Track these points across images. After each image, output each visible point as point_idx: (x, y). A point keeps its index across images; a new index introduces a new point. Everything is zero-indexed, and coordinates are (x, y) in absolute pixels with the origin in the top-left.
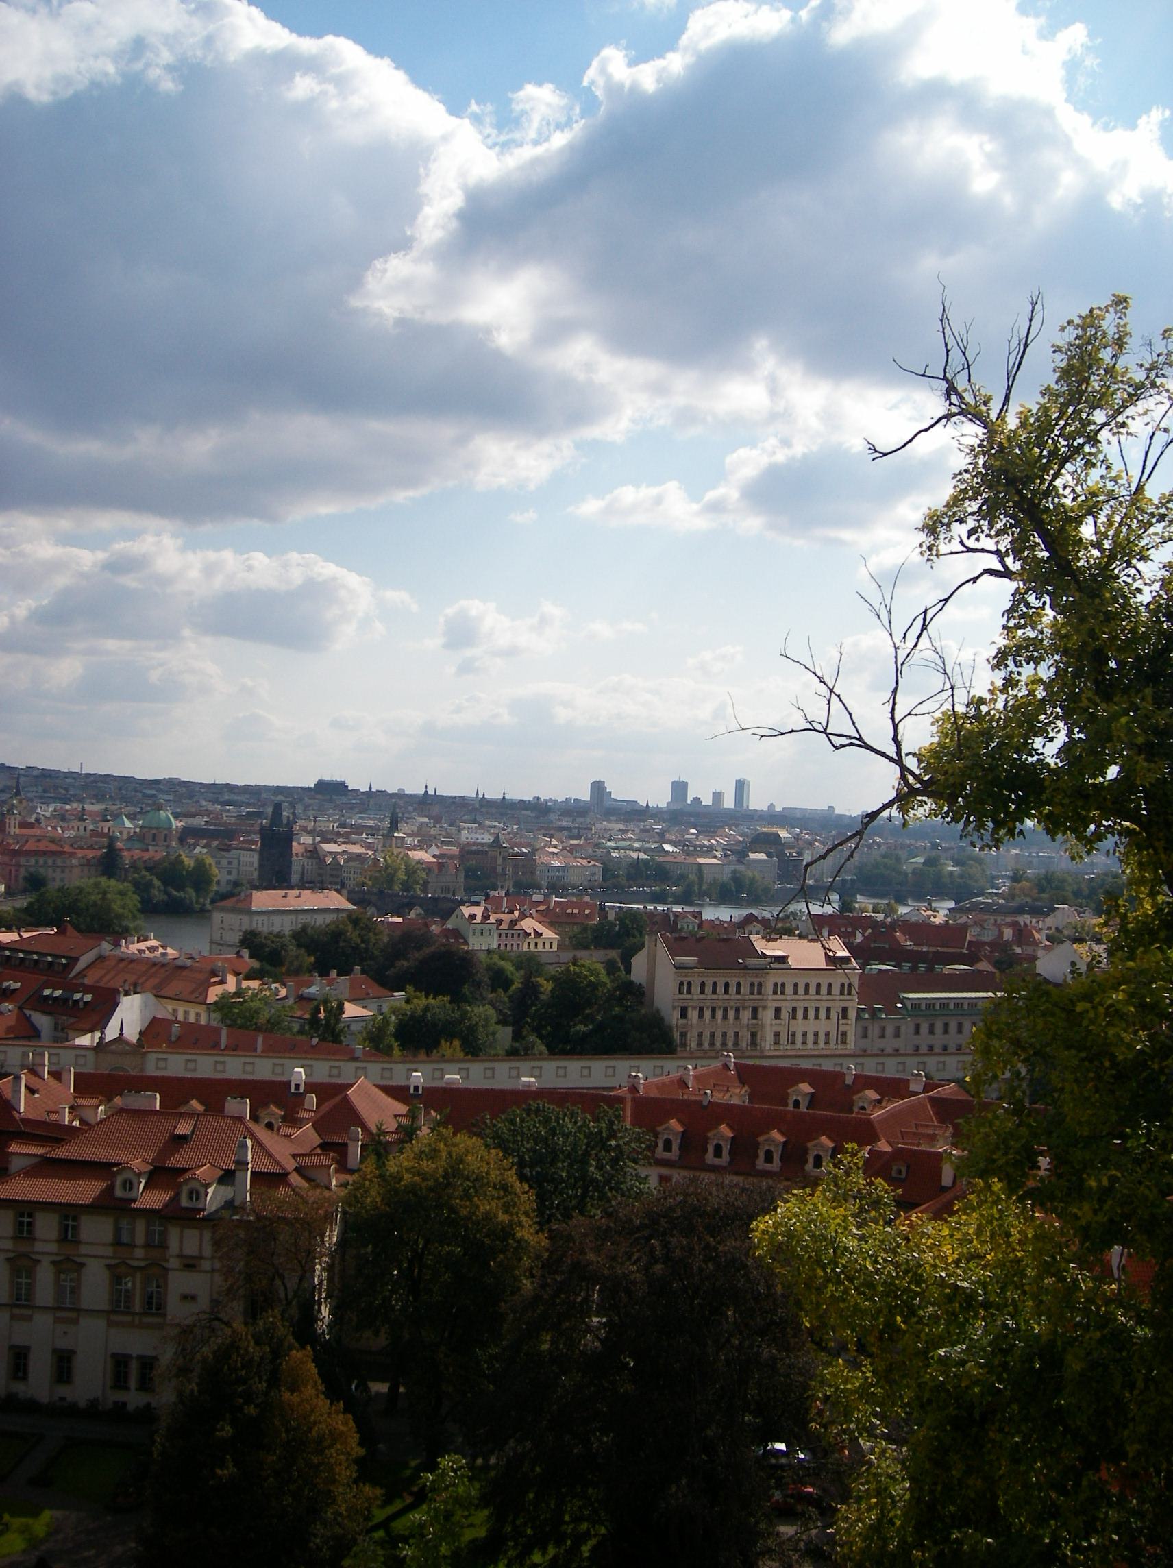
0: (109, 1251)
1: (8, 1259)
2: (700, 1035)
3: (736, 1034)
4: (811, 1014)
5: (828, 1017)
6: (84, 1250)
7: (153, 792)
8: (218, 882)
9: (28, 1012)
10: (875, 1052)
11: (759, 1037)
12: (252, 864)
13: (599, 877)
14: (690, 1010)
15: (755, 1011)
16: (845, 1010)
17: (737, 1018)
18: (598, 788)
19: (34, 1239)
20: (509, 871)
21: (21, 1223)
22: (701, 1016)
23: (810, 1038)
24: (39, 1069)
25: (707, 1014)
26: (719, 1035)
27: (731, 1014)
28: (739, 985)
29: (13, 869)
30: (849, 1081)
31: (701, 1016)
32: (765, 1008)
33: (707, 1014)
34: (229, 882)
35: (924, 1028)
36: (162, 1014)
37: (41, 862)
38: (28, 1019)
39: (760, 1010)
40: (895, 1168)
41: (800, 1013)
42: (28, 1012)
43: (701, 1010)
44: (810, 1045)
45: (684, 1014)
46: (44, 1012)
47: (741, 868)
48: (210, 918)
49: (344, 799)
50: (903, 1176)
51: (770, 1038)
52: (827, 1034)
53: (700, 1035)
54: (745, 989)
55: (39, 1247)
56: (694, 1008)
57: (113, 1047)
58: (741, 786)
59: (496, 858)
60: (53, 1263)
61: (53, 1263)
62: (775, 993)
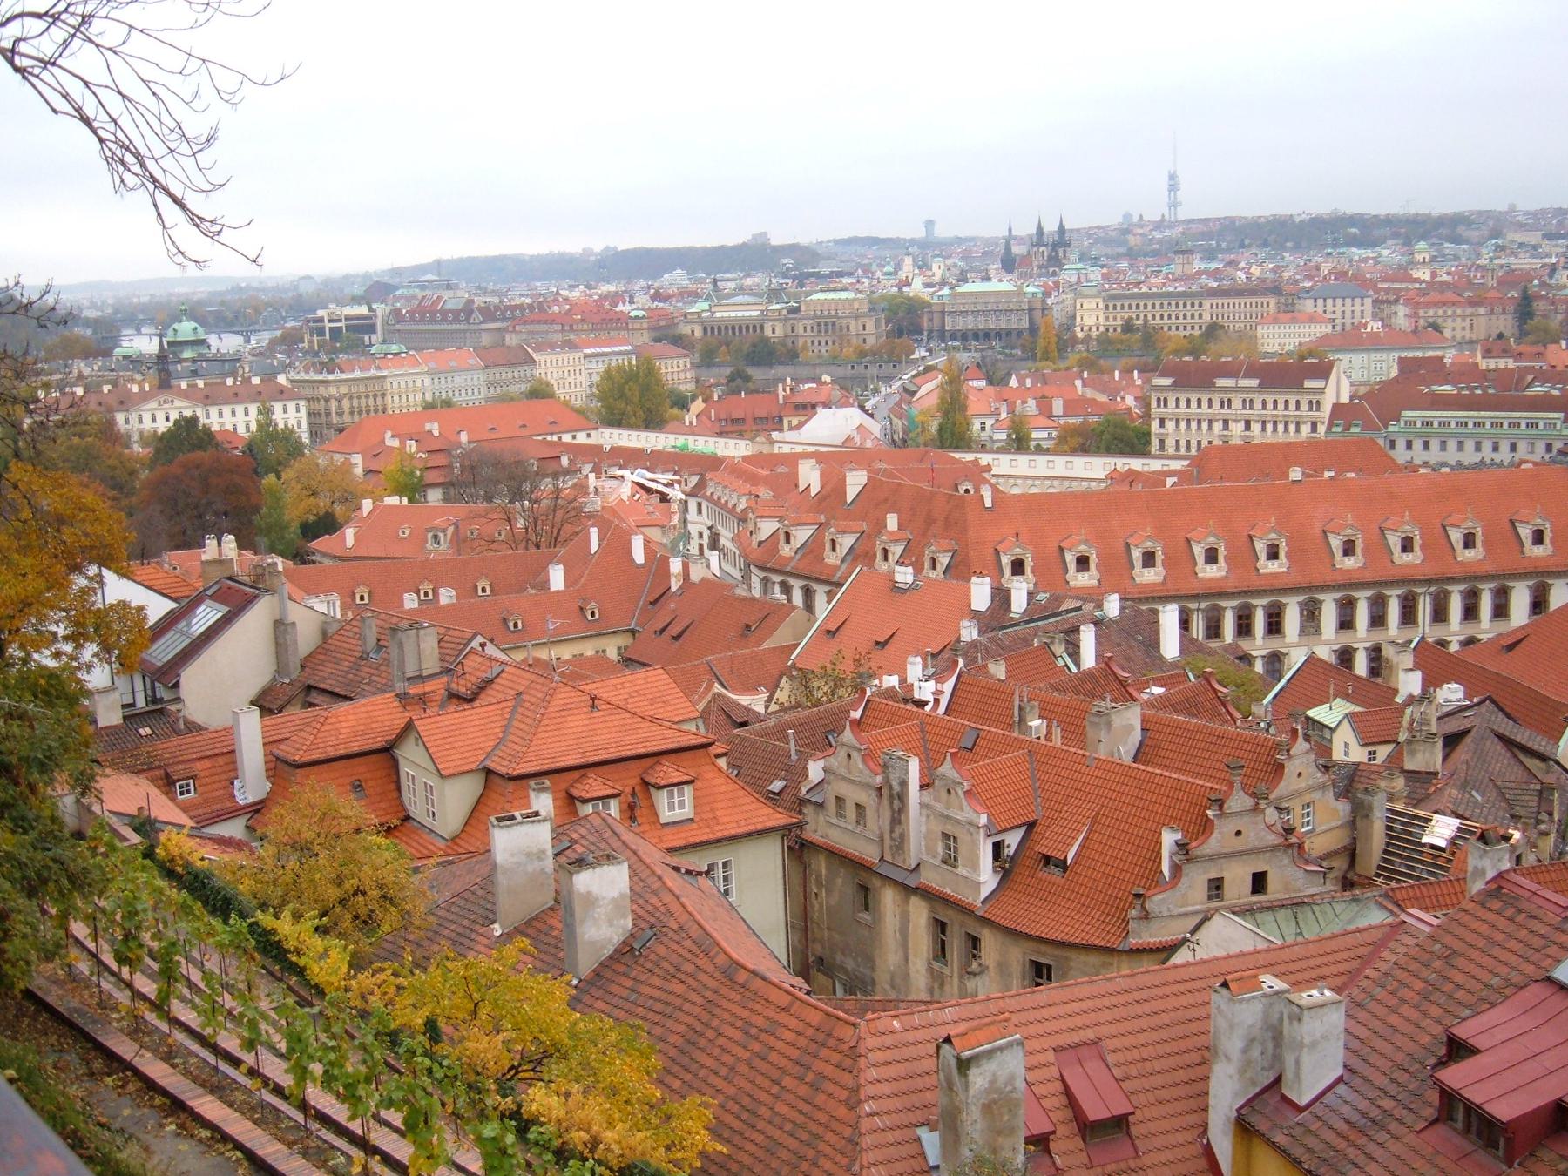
15: (1226, 422)
17: (1210, 428)
25: (1183, 425)
27: (1205, 426)
29: (1413, 320)
33: (1183, 425)
37: (1440, 312)
41: (1269, 427)
43: (1178, 421)
45: (1162, 422)
53: (1178, 442)
54: (1216, 405)
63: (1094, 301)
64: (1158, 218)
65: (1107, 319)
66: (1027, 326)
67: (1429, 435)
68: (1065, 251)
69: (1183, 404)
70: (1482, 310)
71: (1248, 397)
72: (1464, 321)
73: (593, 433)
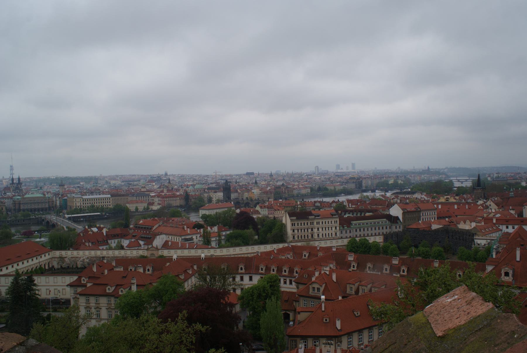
0: (106, 305)
1: (85, 308)
2: (298, 236)
3: (308, 235)
4: (327, 229)
5: (332, 229)
6: (101, 305)
7: (207, 178)
8: (213, 201)
9: (138, 241)
10: (345, 237)
11: (314, 235)
12: (222, 195)
13: (309, 191)
14: (295, 230)
15: (312, 230)
16: (336, 227)
17: (308, 231)
18: (317, 167)
19: (90, 303)
20: (286, 192)
21: (87, 299)
22: (298, 231)
23: (327, 234)
24: (104, 261)
25: (300, 231)
26: (306, 235)
27: (306, 230)
28: (307, 223)
30: (318, 249)
31: (298, 231)
32: (315, 228)
33: (300, 231)
34: (216, 200)
35: (358, 230)
36: (168, 239)
38: (139, 242)
39: (313, 229)
40: (305, 275)
41: (324, 229)
42: (138, 241)
44: (327, 236)
45: (294, 231)
46: (142, 241)
47: (346, 186)
48: (199, 211)
49: (253, 176)
50: (307, 277)
51: (316, 235)
52: (332, 234)
53: (298, 236)
54: (309, 224)
55: (91, 305)
56: (296, 229)
57: (151, 249)
58: (353, 165)
59: (282, 189)
60: (95, 308)
61: (95, 308)
62: (317, 224)
63: (79, 199)
64: (8, 177)
65: (83, 204)
66: (48, 207)
67: (361, 227)
68: (20, 186)
69: (300, 225)
70: (178, 198)
71: (318, 221)
72: (175, 201)
73: (50, 253)
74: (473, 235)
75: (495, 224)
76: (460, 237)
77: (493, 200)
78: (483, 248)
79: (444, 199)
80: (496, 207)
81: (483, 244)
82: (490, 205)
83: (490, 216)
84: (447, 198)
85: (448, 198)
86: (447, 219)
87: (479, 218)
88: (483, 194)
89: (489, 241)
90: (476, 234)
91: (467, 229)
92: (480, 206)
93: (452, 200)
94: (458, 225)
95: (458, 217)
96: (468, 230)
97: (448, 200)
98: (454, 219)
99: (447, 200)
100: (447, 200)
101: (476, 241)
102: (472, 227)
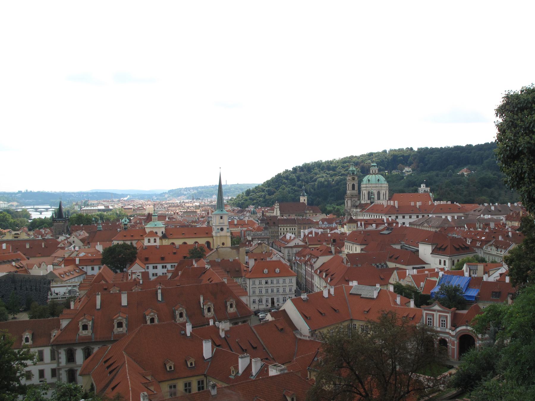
74: (49, 283)
75: (77, 266)
76: (31, 286)
77: (78, 234)
78: (62, 298)
79: (12, 236)
80: (81, 244)
81: (62, 293)
82: (74, 242)
83: (71, 256)
84: (16, 234)
85: (18, 234)
86: (14, 264)
87: (58, 260)
88: (65, 228)
89: (70, 288)
90: (53, 280)
91: (41, 275)
92: (61, 244)
93: (24, 236)
94: (30, 271)
95: (30, 259)
96: (43, 275)
97: (17, 237)
98: (24, 263)
99: (15, 237)
100: (15, 237)
101: (52, 289)
102: (49, 272)
